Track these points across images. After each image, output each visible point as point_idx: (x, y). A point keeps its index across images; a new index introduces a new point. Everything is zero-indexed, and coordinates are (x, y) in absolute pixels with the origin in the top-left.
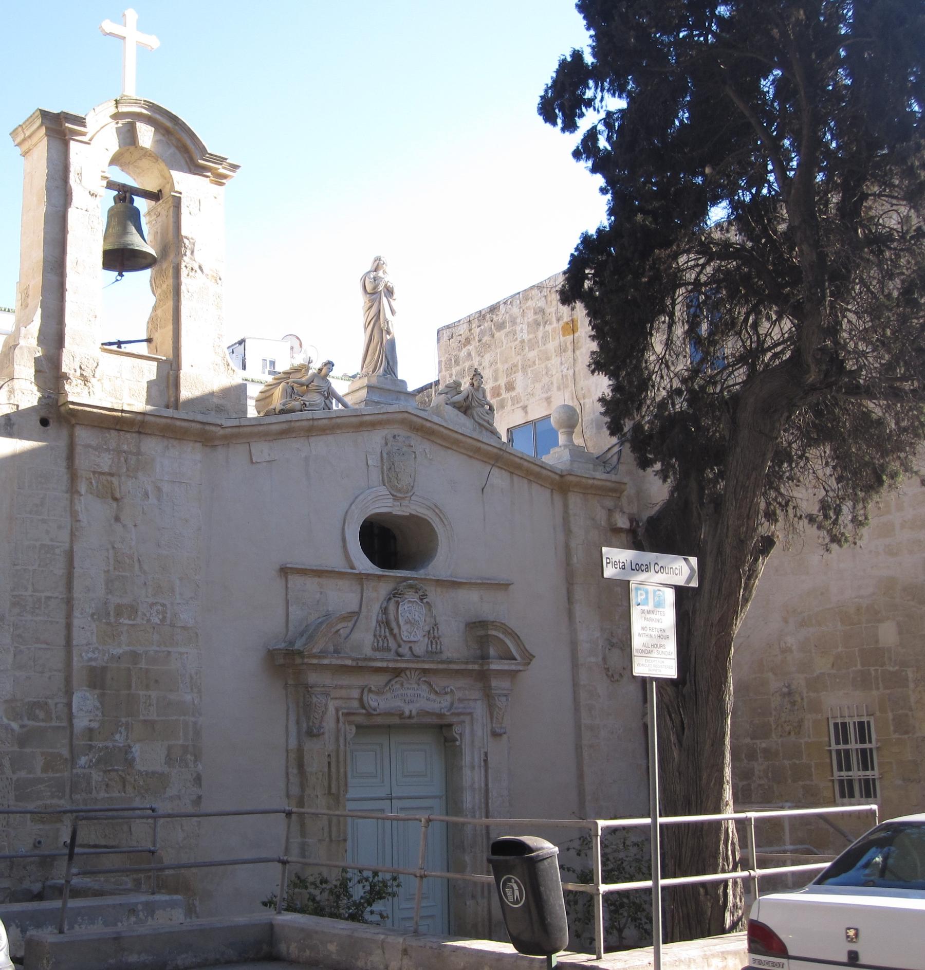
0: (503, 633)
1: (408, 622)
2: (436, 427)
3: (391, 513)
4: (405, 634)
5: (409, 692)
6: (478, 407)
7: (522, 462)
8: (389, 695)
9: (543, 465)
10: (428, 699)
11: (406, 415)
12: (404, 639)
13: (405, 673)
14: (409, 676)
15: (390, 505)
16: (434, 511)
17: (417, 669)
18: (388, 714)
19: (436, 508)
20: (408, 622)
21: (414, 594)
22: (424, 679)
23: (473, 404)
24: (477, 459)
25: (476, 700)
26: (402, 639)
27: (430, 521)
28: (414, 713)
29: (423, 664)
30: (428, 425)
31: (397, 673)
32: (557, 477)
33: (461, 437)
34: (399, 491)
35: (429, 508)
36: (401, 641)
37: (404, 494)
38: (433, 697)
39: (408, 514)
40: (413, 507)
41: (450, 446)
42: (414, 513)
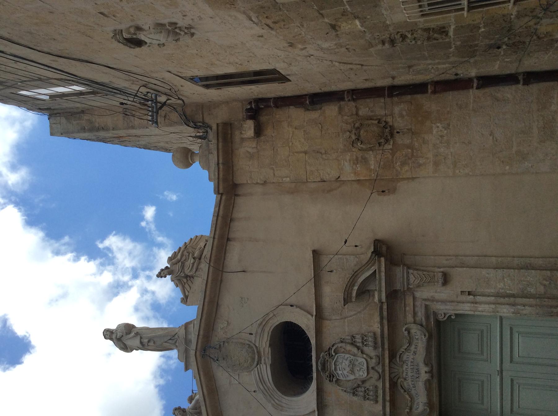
0: (354, 285)
1: (352, 372)
2: (203, 325)
3: (271, 365)
4: (361, 373)
5: (410, 374)
6: (184, 272)
7: (217, 237)
8: (413, 392)
9: (216, 215)
10: (415, 353)
11: (198, 353)
12: (366, 374)
13: (394, 378)
14: (396, 374)
15: (265, 366)
16: (264, 325)
17: (390, 367)
18: (429, 390)
19: (262, 325)
20: (352, 372)
21: (329, 363)
22: (398, 359)
23: (183, 275)
24: (222, 277)
25: (414, 298)
26: (366, 377)
27: (272, 328)
28: (426, 369)
29: (386, 365)
30: (201, 332)
31: (393, 385)
32: (224, 197)
33: (207, 300)
34: (253, 359)
35: (263, 330)
36: (367, 377)
37: (255, 353)
38: (413, 348)
39: (270, 349)
40: (264, 346)
41: (216, 304)
42: (268, 345)
